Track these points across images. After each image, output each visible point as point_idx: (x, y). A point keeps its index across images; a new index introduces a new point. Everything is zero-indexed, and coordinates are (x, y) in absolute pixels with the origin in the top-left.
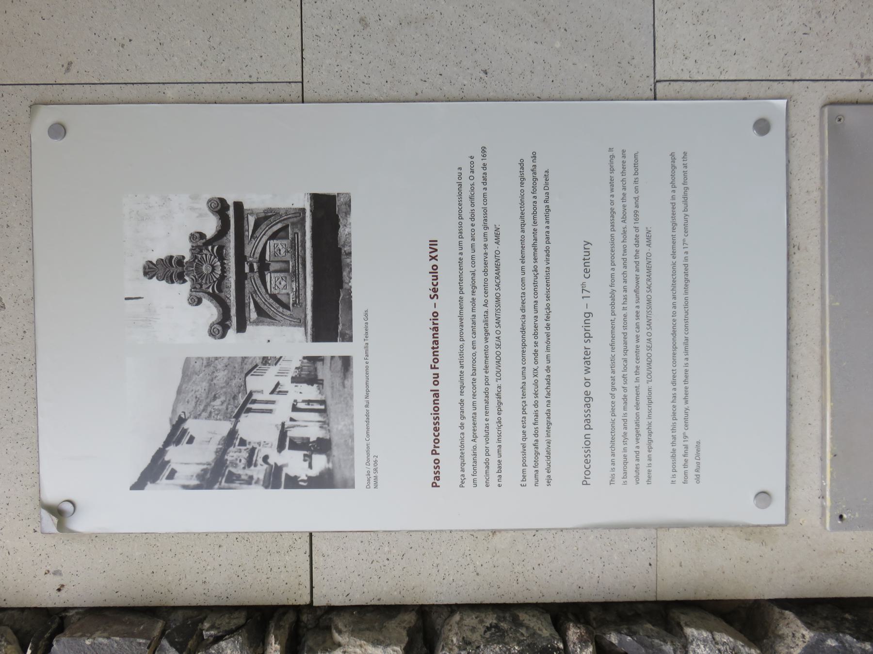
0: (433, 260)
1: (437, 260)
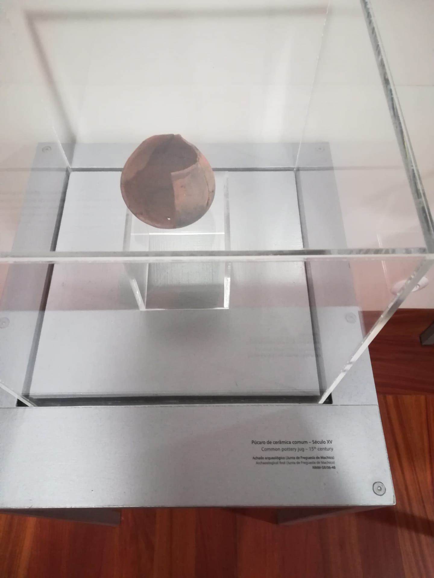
0: (327, 442)
1: (327, 443)
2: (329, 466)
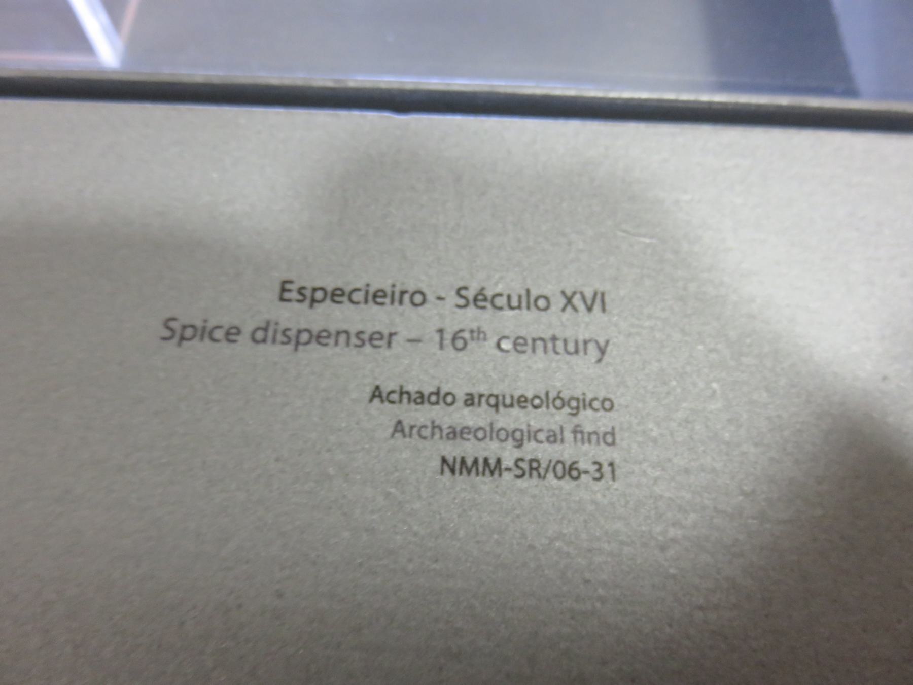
0: (563, 301)
1: (564, 310)
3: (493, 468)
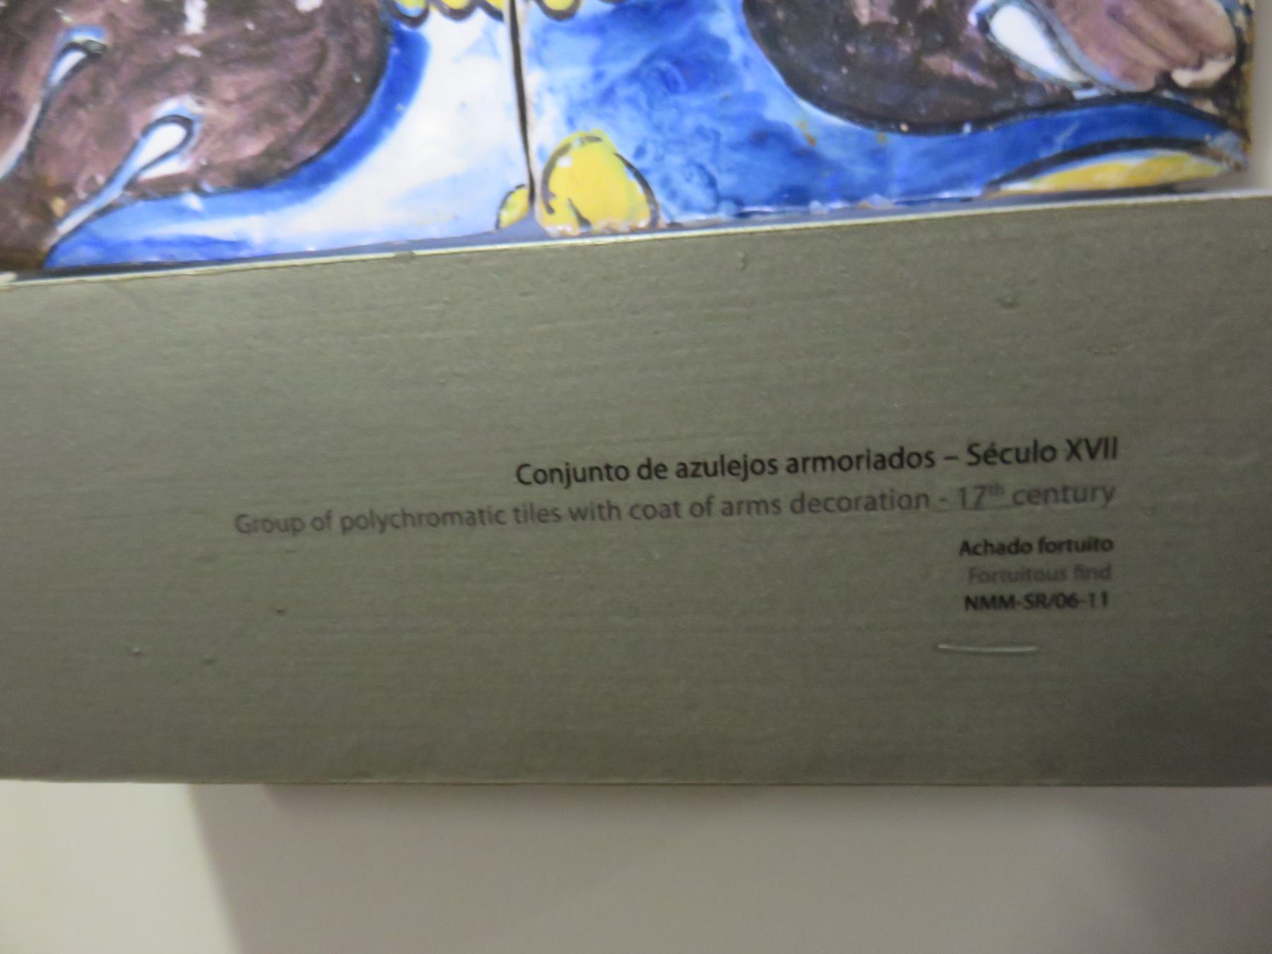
1: (1068, 458)
2: (1068, 592)
3: (1006, 603)
